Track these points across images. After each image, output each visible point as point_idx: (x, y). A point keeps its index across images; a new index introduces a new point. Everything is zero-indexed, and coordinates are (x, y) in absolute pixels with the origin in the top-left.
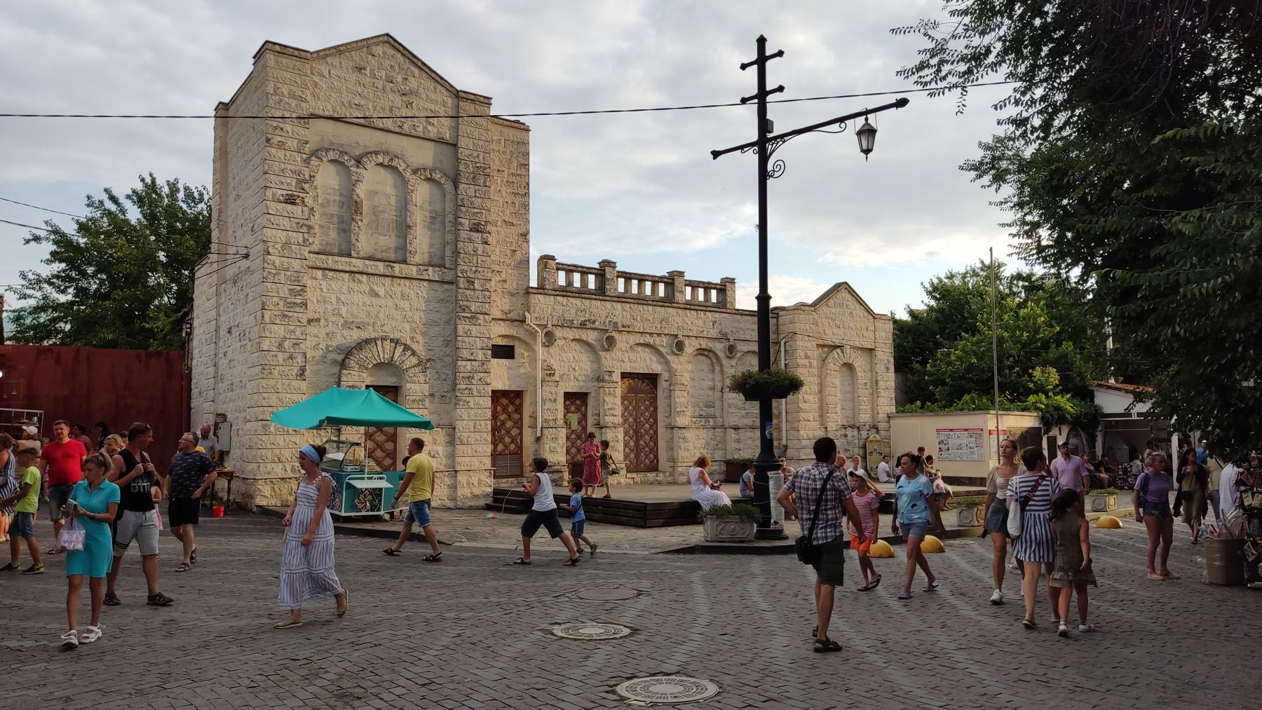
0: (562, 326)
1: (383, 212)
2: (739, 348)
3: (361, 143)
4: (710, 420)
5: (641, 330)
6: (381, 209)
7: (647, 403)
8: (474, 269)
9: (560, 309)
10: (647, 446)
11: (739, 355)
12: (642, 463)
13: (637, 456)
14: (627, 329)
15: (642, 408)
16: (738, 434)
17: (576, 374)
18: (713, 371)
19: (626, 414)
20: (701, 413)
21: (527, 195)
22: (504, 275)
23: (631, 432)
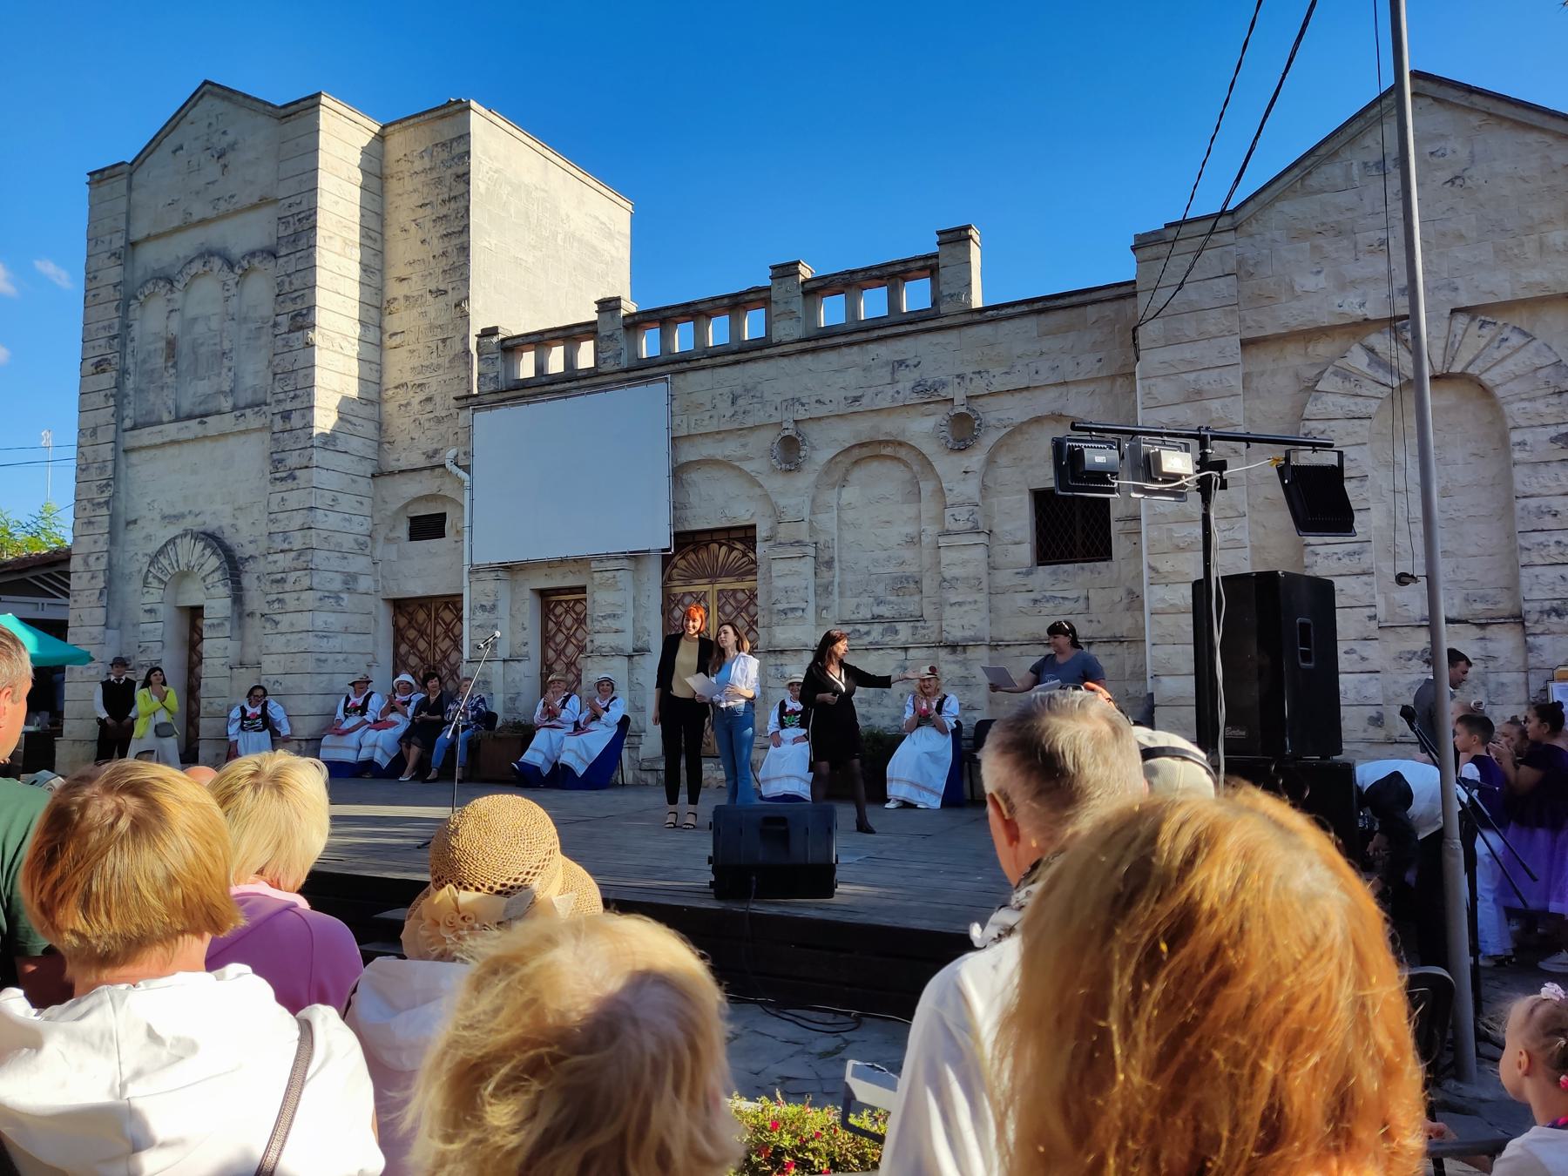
1: (202, 344)
2: (991, 418)
3: (181, 256)
4: (899, 626)
6: (200, 341)
8: (292, 394)
11: (988, 440)
16: (964, 663)
20: (878, 610)
21: (466, 229)
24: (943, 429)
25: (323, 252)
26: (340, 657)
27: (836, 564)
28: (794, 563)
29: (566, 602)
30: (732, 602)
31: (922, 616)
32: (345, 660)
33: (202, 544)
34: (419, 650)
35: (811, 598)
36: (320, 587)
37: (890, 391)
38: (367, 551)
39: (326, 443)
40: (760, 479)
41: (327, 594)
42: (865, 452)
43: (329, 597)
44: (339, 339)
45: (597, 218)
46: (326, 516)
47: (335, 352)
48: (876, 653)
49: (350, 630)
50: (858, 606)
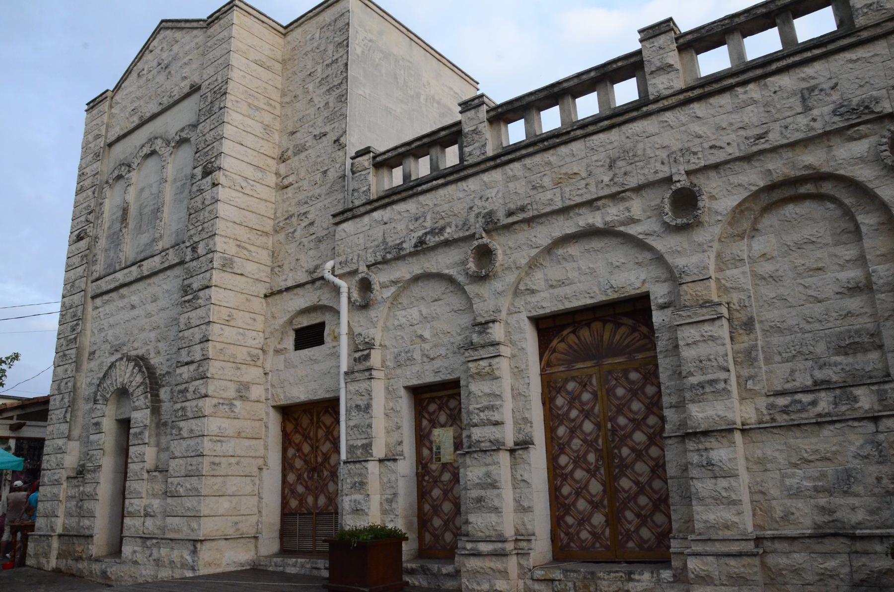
0: (385, 262)
4: (859, 392)
5: (559, 205)
6: (145, 204)
7: (634, 376)
8: (200, 228)
9: (378, 233)
10: (641, 490)
12: (629, 537)
13: (613, 520)
14: (521, 216)
15: (620, 392)
17: (427, 346)
18: (857, 233)
19: (574, 413)
20: (819, 375)
22: (311, 216)
23: (591, 458)
24: (883, 148)
25: (230, 111)
26: (233, 460)
27: (757, 326)
28: (707, 327)
29: (440, 398)
30: (625, 383)
31: (889, 375)
32: (238, 464)
33: (133, 364)
34: (303, 453)
35: (732, 367)
36: (216, 394)
37: (802, 121)
38: (259, 363)
39: (224, 266)
40: (650, 241)
41: (221, 401)
42: (776, 195)
43: (223, 404)
44: (240, 180)
45: (451, 89)
46: (222, 329)
47: (237, 190)
48: (832, 427)
49: (243, 435)
50: (793, 372)
